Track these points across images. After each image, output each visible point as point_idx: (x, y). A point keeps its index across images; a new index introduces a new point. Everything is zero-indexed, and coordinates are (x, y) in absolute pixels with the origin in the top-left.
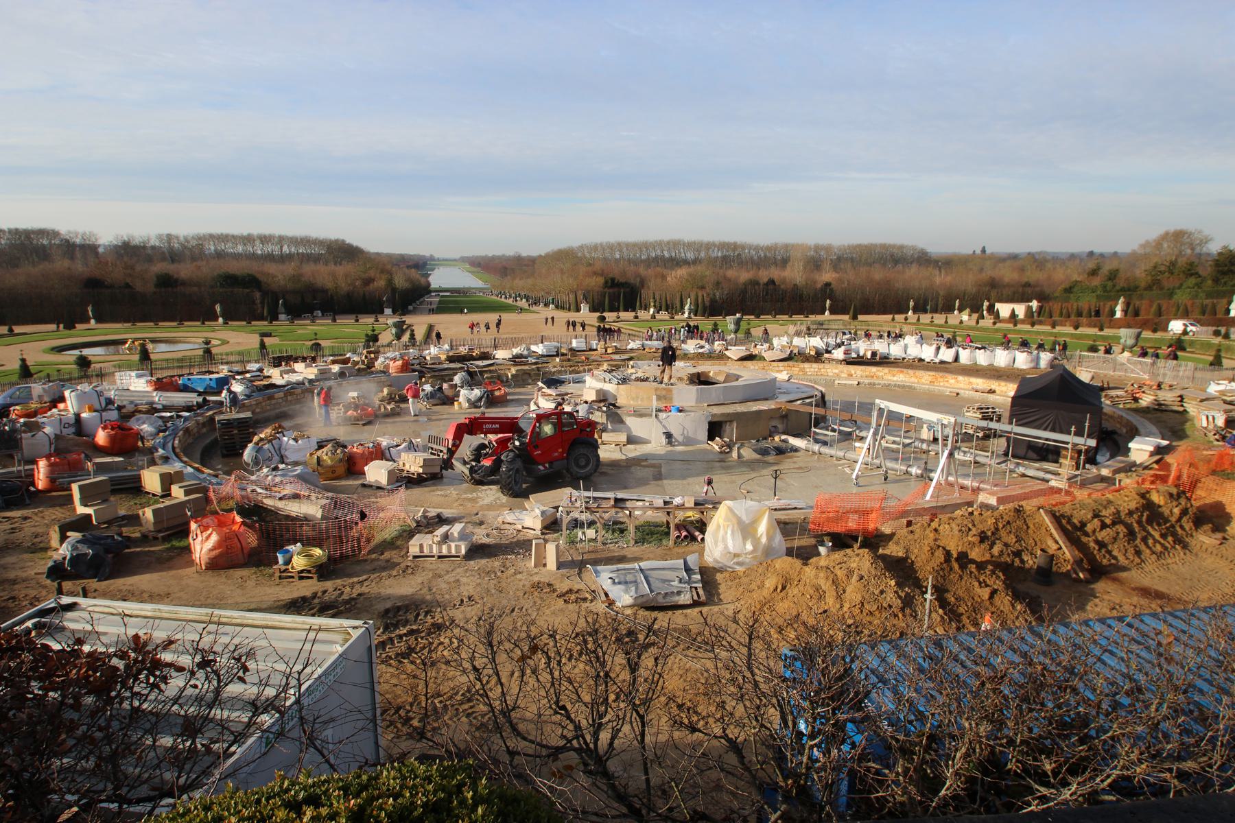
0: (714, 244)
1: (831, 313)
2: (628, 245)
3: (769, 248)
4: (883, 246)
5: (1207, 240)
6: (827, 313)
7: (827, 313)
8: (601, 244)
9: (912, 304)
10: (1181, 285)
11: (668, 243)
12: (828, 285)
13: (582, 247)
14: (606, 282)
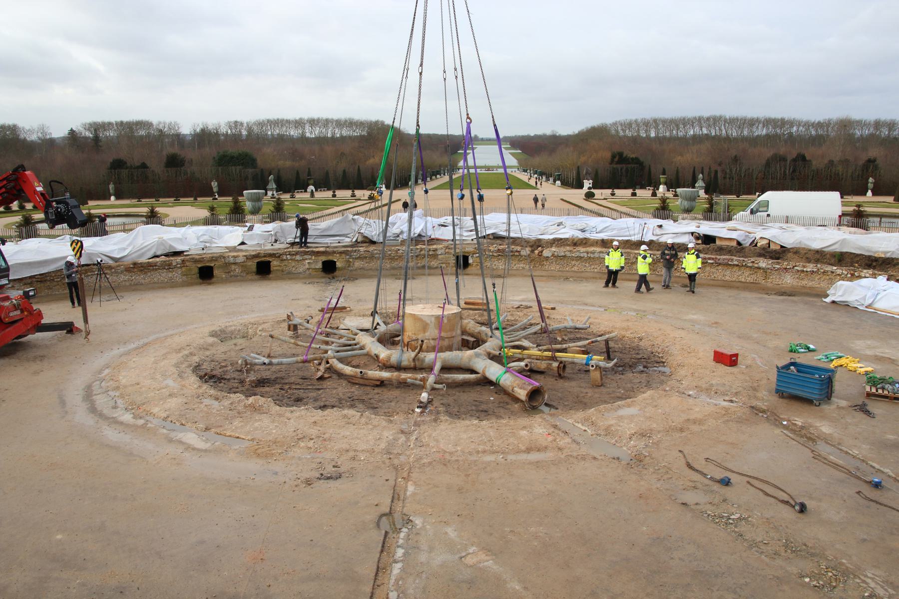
1: (874, 194)
2: (664, 121)
6: (869, 193)
7: (869, 193)
8: (636, 121)
11: (708, 119)
12: (871, 161)
13: (615, 124)
14: (613, 157)
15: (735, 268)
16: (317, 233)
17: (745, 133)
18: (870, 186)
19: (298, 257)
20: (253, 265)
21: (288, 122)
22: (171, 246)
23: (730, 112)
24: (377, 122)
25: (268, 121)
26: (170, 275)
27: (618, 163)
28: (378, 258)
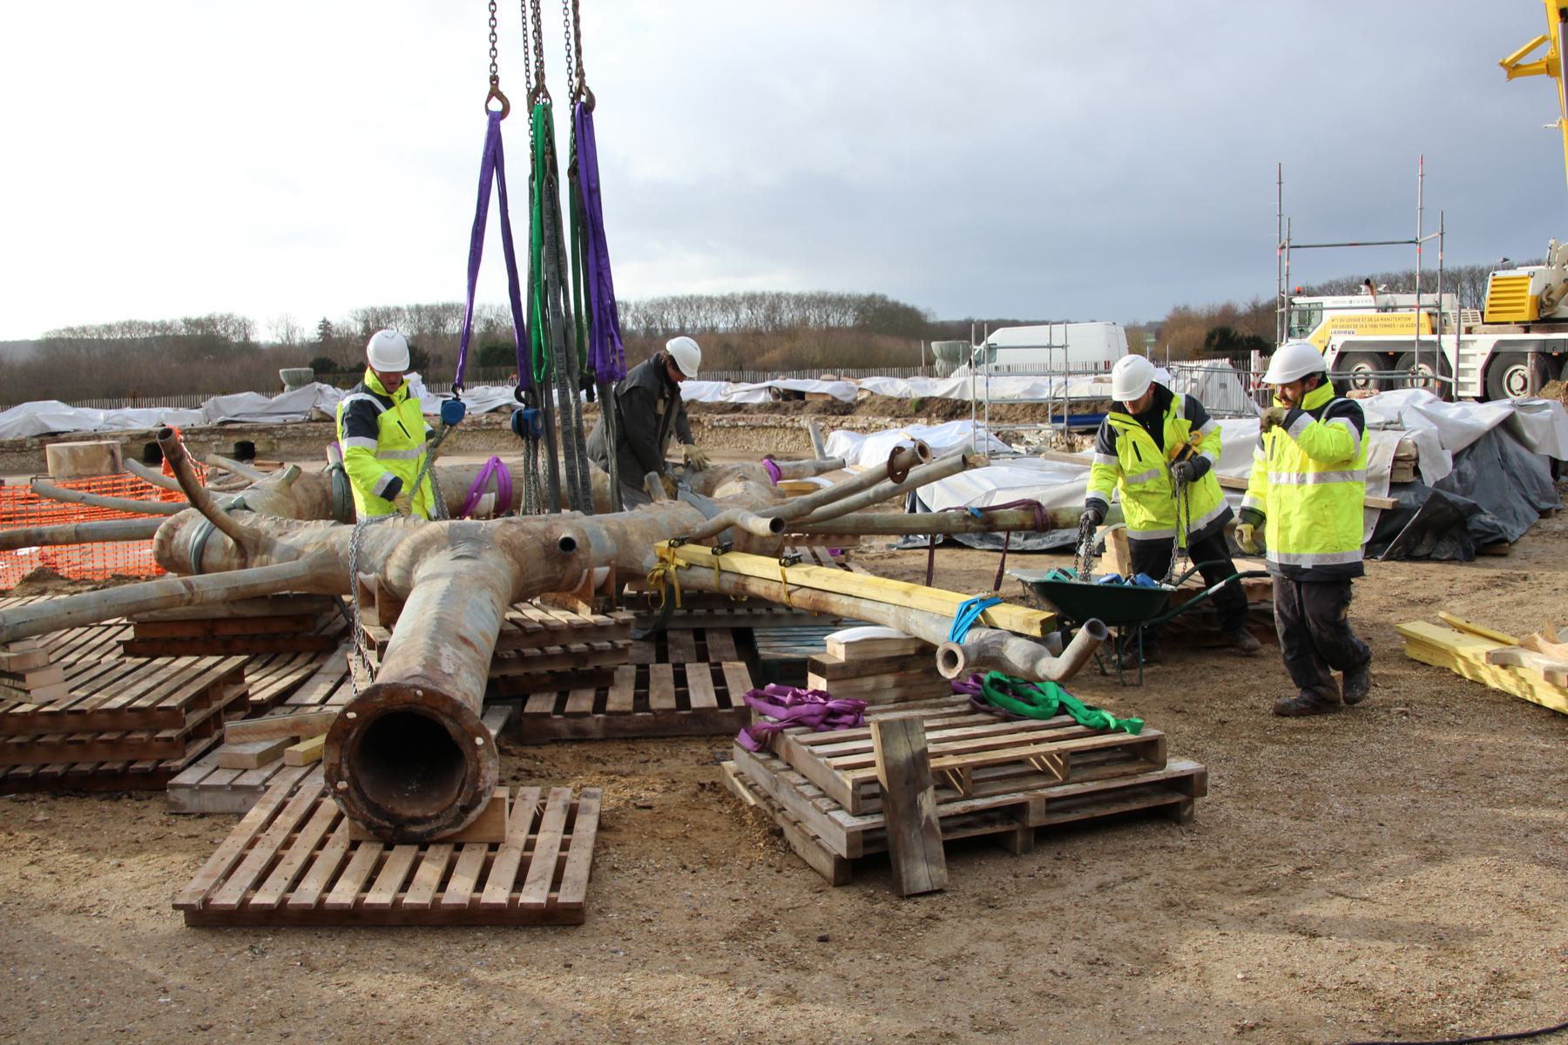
15: (773, 432)
16: (260, 409)
19: (202, 438)
20: (140, 447)
21: (710, 300)
22: (44, 425)
24: (871, 300)
25: (674, 300)
26: (23, 460)
28: (312, 438)
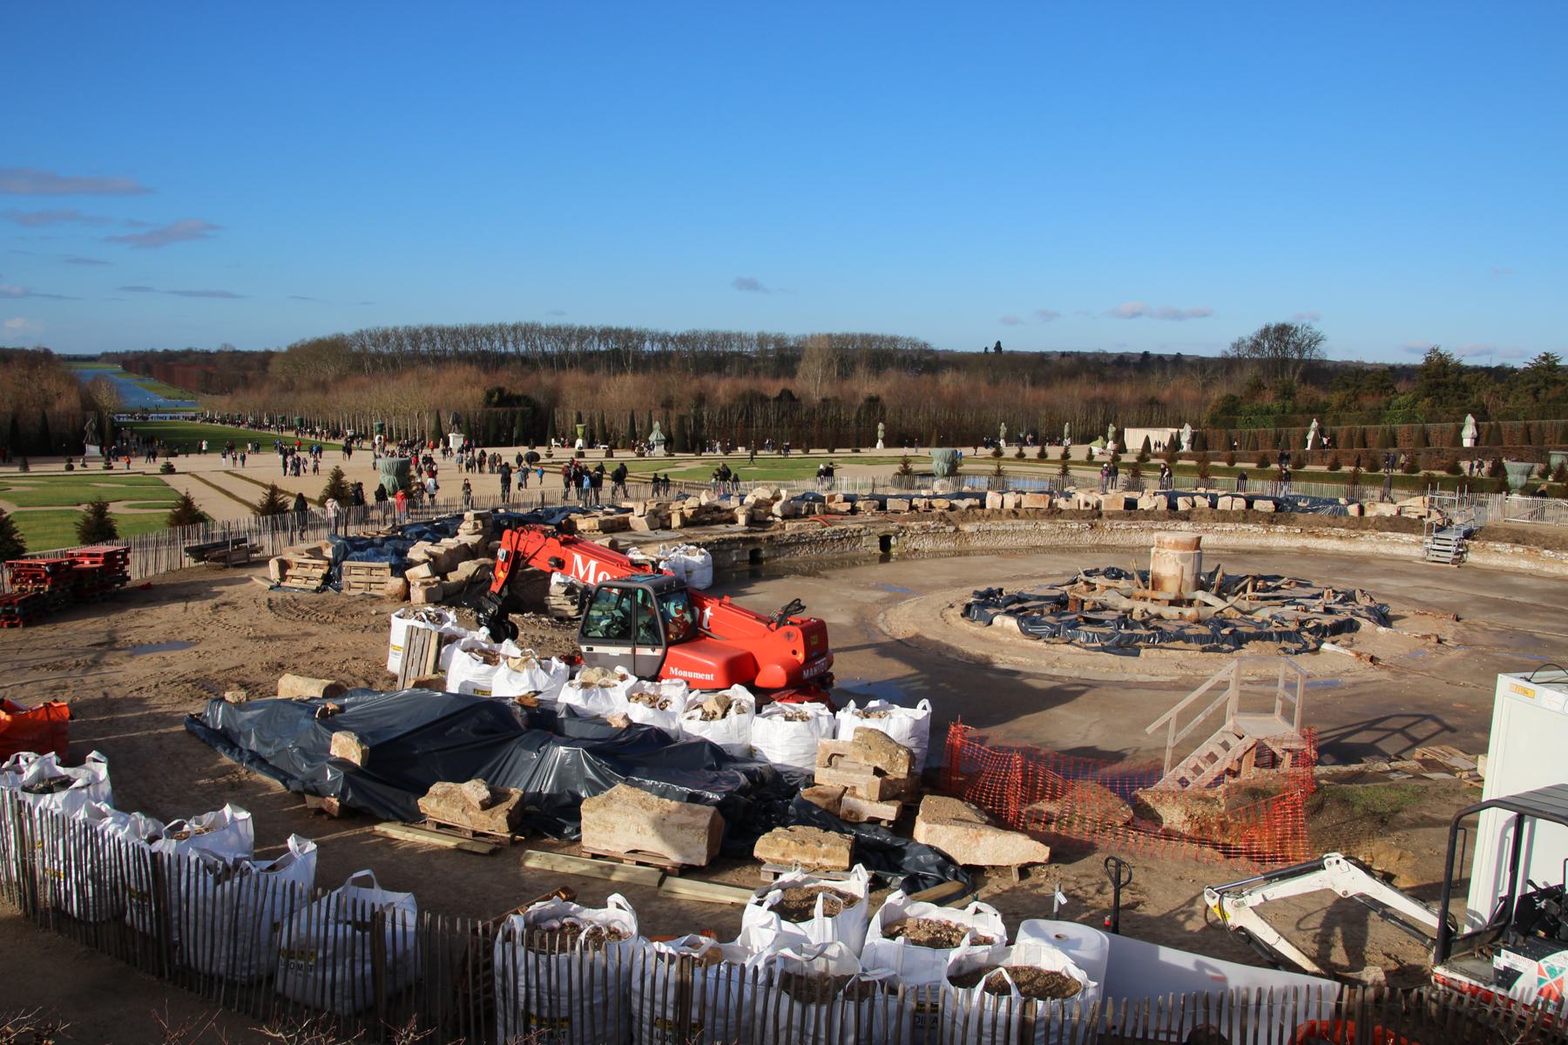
0: (592, 332)
2: (441, 332)
3: (683, 339)
4: (866, 338)
5: (1316, 340)
6: (880, 444)
7: (880, 444)
8: (395, 330)
9: (1003, 429)
10: (1389, 404)
11: (515, 328)
13: (360, 335)
14: (490, 395)
17: (573, 347)
18: (880, 434)
23: (546, 321)
27: (498, 405)
